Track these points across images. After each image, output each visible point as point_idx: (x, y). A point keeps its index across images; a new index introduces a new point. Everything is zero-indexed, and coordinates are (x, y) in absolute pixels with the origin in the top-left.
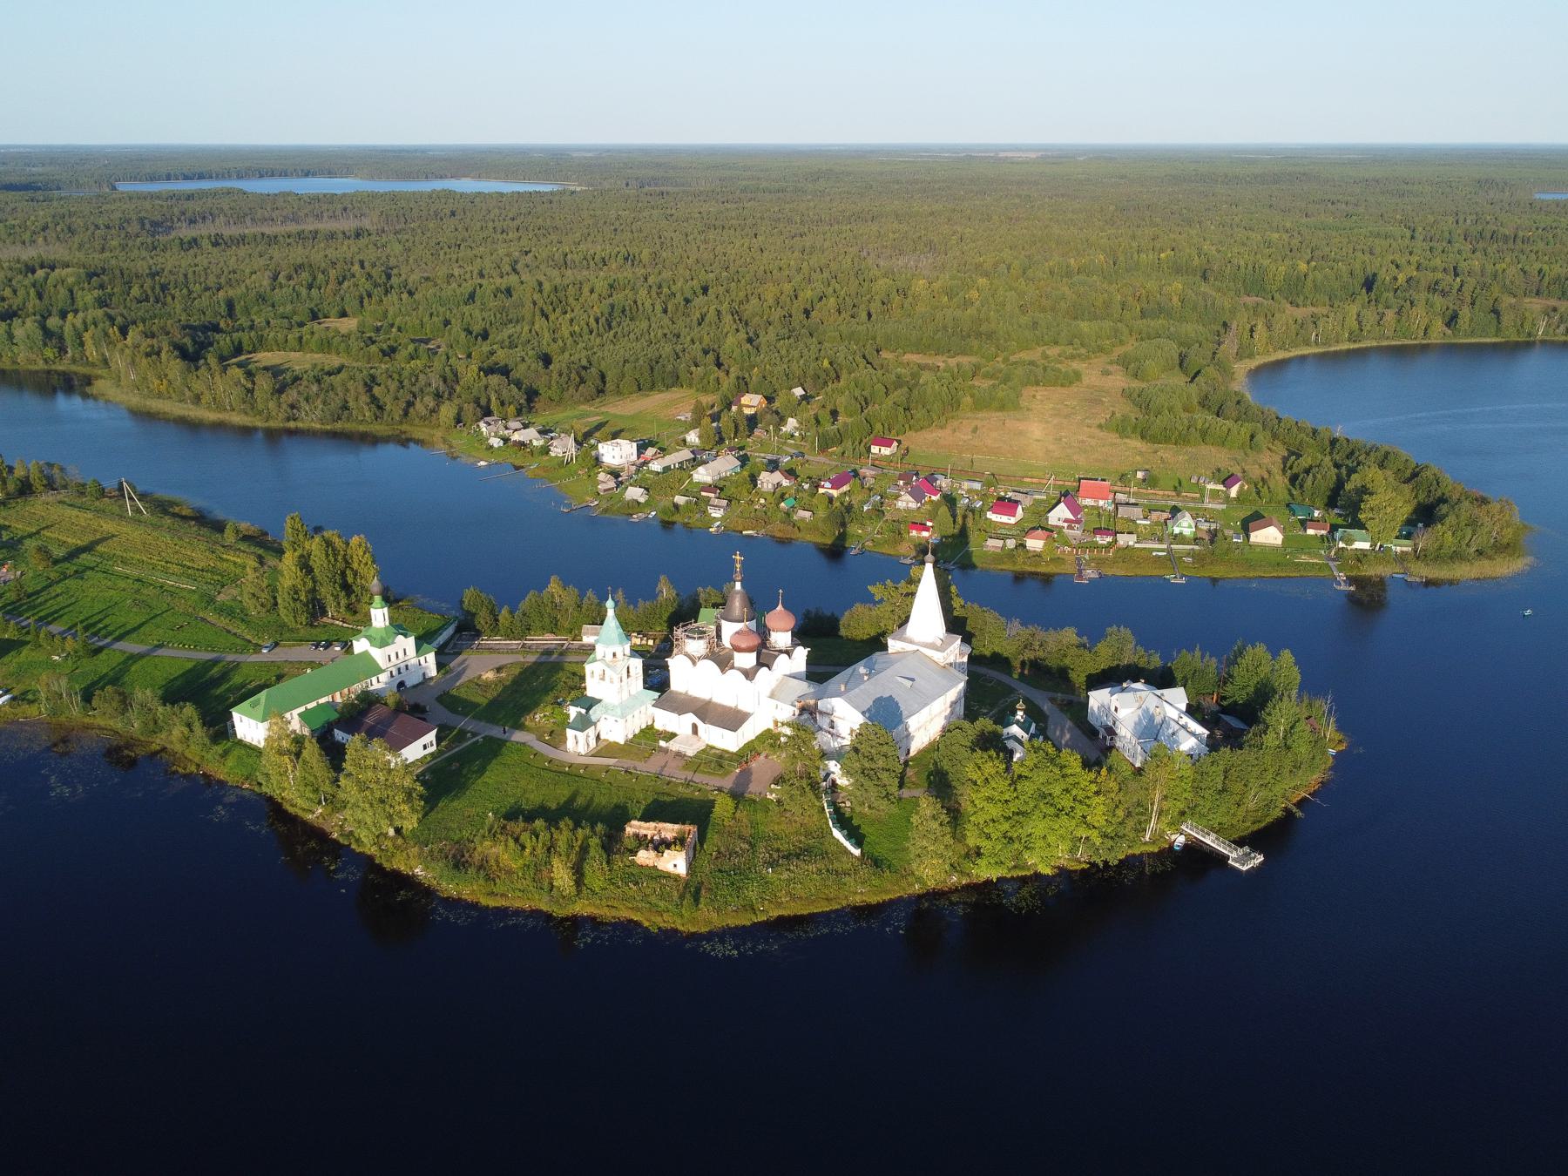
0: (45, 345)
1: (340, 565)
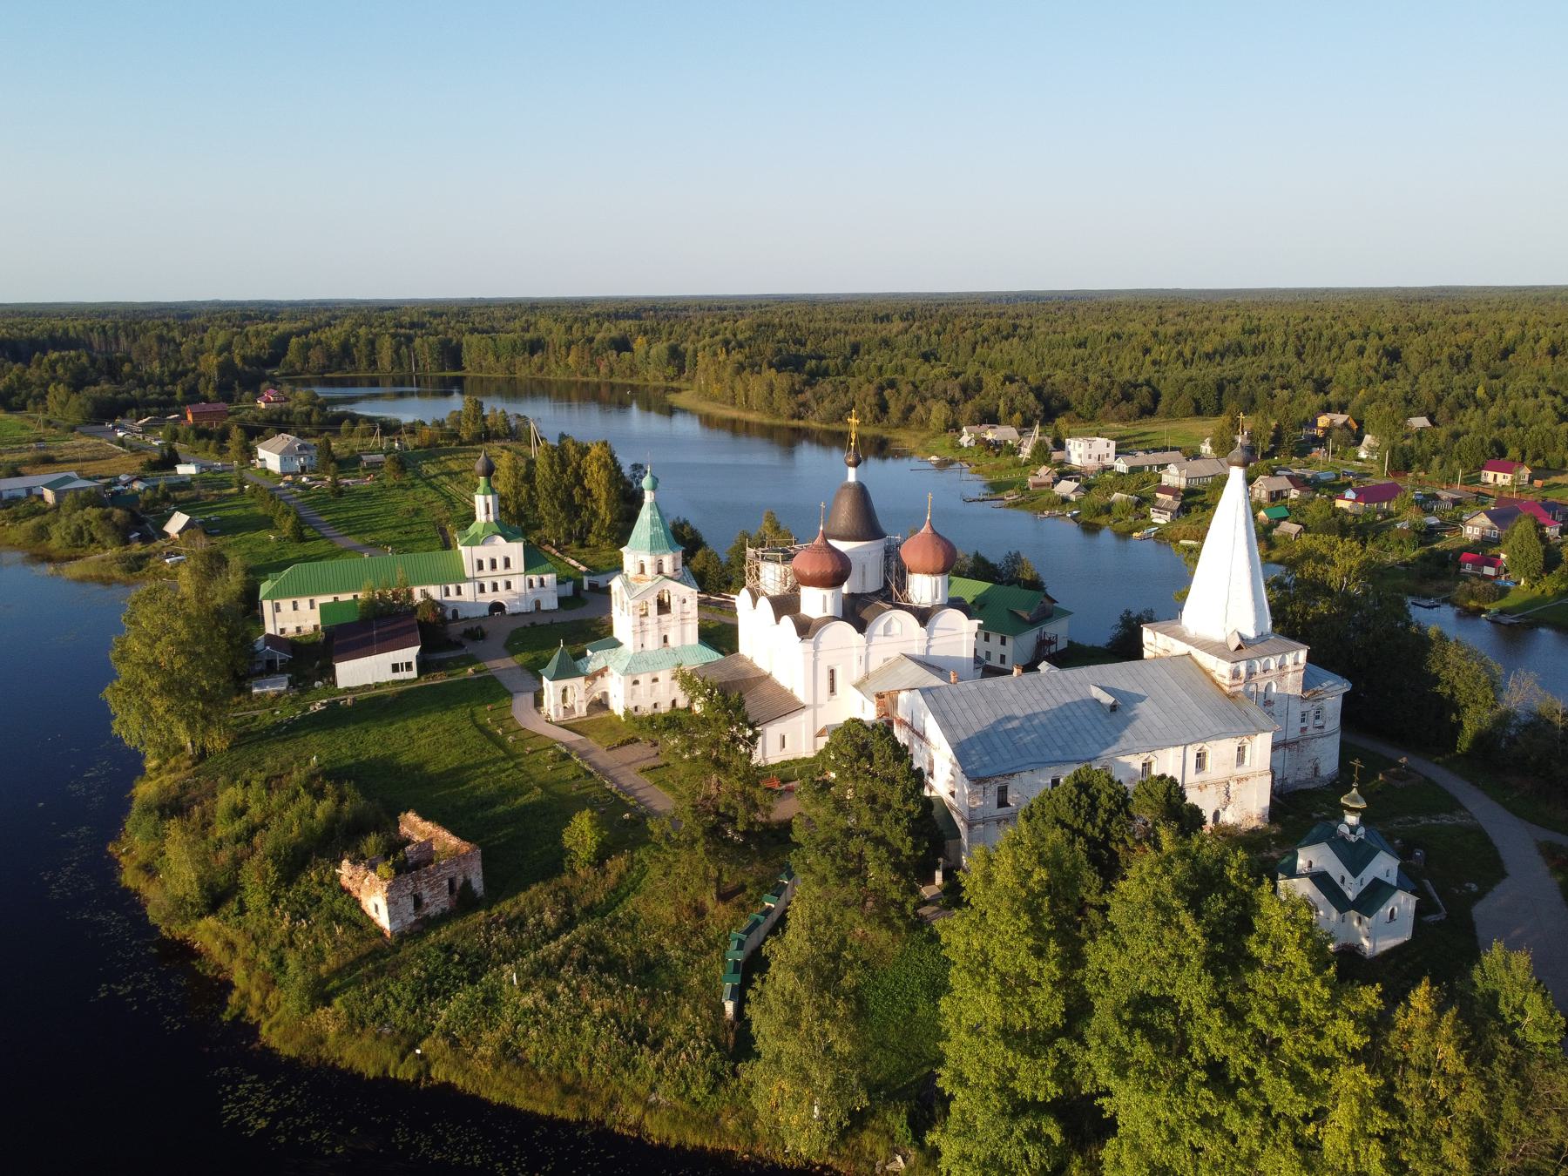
0: (669, 363)
1: (568, 478)
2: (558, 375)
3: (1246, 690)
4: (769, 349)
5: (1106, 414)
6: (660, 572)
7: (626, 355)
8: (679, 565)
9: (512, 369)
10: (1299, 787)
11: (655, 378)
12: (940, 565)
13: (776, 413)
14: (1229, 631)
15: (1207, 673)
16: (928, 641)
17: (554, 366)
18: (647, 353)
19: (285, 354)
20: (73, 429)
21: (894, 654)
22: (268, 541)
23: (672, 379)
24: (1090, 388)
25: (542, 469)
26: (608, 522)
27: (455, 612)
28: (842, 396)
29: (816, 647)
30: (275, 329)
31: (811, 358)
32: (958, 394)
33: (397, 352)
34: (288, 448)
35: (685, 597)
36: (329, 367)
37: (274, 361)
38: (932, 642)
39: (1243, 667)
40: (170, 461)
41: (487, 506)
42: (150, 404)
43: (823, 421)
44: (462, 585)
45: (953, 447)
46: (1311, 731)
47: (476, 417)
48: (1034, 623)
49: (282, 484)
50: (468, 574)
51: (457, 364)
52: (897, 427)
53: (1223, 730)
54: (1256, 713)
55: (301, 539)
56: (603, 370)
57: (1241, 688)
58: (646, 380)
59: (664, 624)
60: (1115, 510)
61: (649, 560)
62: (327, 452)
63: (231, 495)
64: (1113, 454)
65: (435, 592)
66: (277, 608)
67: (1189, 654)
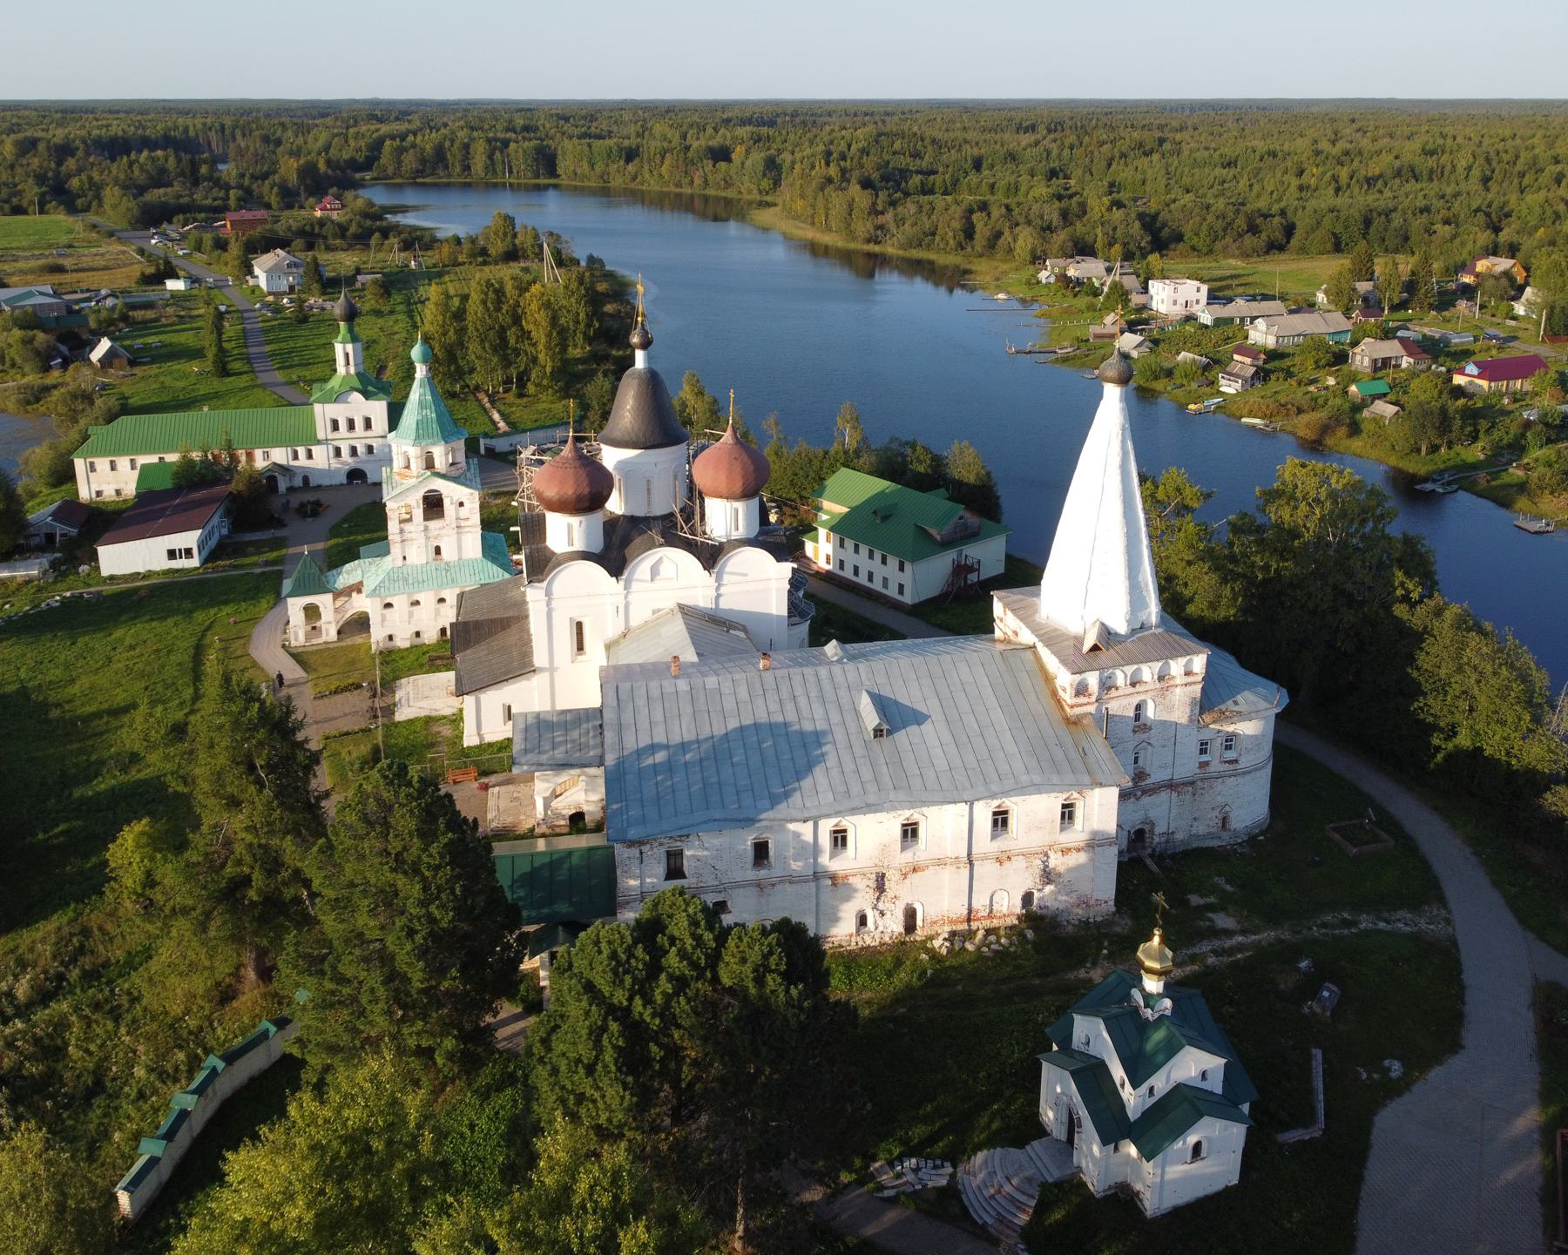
1: (504, 318)
2: (652, 184)
3: (1099, 710)
4: (870, 162)
5: (1226, 247)
6: (429, 464)
7: (722, 165)
8: (461, 457)
9: (605, 177)
10: (1195, 845)
11: (750, 192)
12: (738, 487)
13: (851, 235)
14: (1090, 620)
15: (1048, 679)
16: (718, 588)
17: (647, 176)
18: (743, 164)
19: (378, 158)
20: (111, 234)
21: (669, 603)
22: (186, 376)
23: (767, 194)
24: (1210, 218)
25: (474, 307)
26: (548, 370)
27: (306, 479)
28: (925, 218)
29: (548, 593)
30: (377, 130)
31: (918, 172)
32: (1055, 218)
33: (491, 157)
34: (276, 265)
35: (464, 501)
36: (422, 171)
37: (367, 165)
38: (722, 590)
39: (1092, 679)
40: (158, 279)
41: (347, 355)
42: (201, 209)
43: (902, 247)
44: (313, 448)
45: (1028, 283)
46: (1216, 766)
47: (505, 234)
48: (946, 544)
49: (258, 306)
50: (321, 435)
51: (552, 172)
52: (981, 256)
53: (1037, 779)
54: (1099, 748)
55: (223, 371)
56: (697, 181)
57: (1092, 709)
58: (740, 192)
59: (433, 533)
60: (1177, 373)
61: (414, 452)
62: (316, 268)
63: (198, 316)
64: (1204, 300)
65: (280, 455)
66: (92, 468)
67: (1034, 647)
